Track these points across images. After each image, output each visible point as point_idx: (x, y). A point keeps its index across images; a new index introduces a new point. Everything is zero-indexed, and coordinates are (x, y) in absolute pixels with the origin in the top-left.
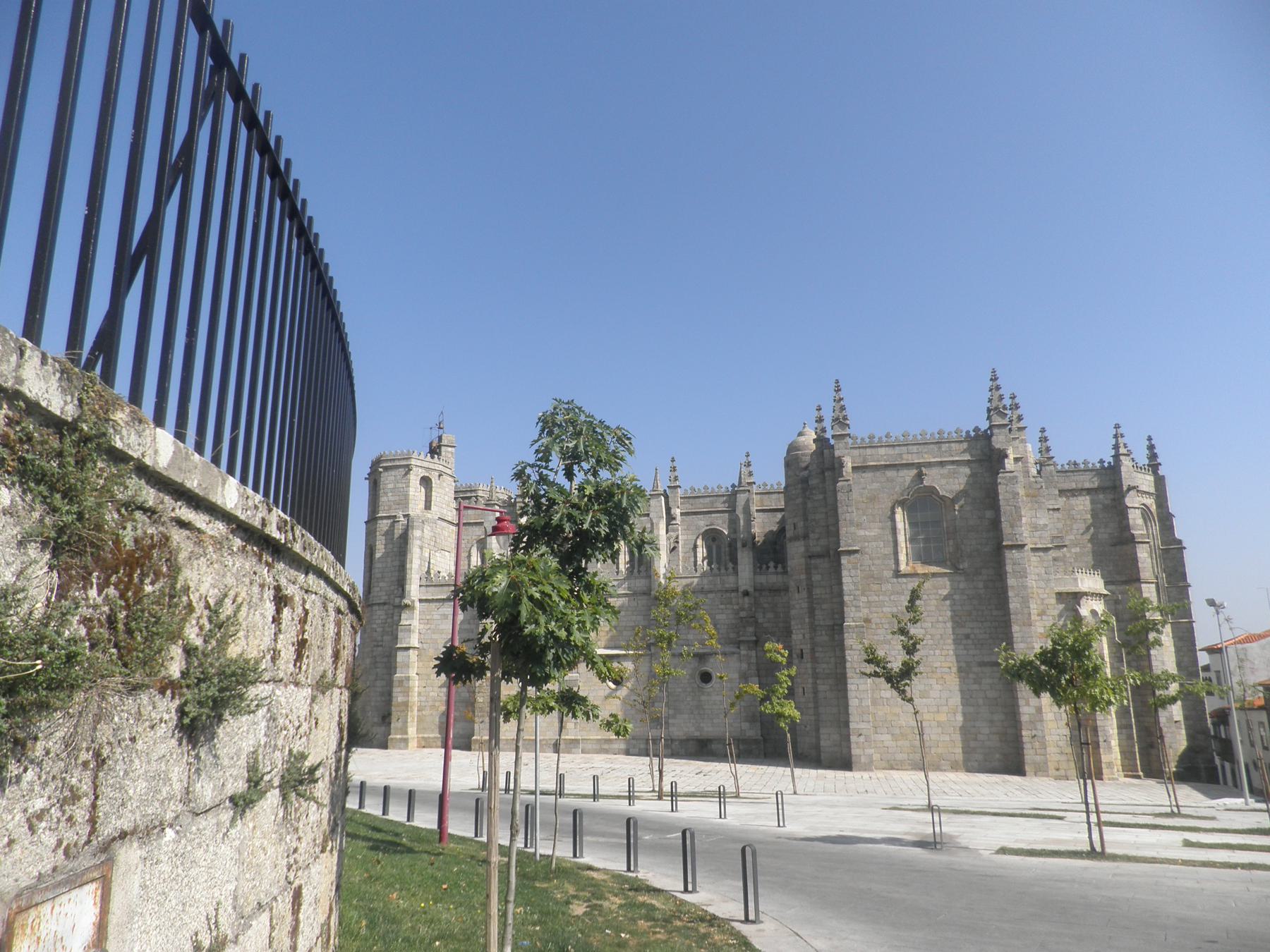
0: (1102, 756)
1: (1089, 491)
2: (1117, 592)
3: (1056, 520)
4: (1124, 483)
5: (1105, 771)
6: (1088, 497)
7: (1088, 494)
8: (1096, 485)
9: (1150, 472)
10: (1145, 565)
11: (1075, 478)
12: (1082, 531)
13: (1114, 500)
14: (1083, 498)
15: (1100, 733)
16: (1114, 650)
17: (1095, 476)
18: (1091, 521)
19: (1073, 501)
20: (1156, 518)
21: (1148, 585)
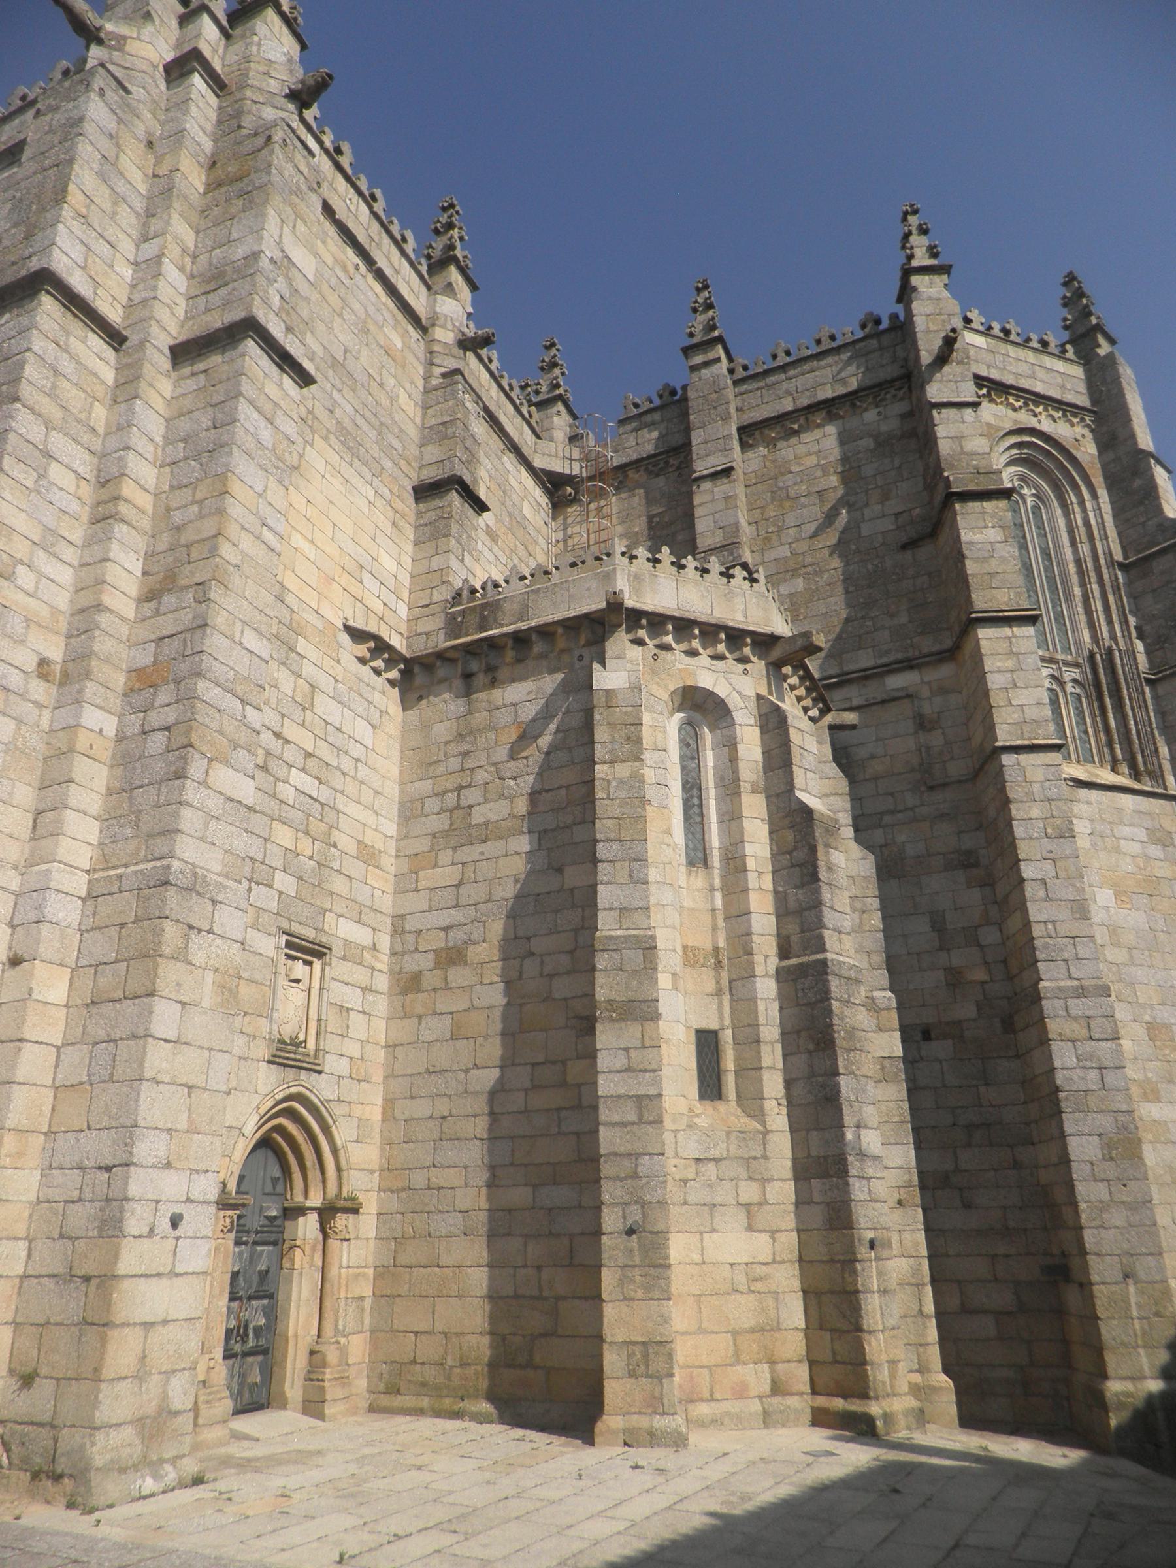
0: (610, 1311)
1: (829, 408)
2: (925, 692)
3: (721, 505)
4: (921, 344)
5: (615, 1390)
6: (831, 429)
7: (831, 417)
8: (853, 384)
9: (1070, 354)
10: (993, 566)
11: (791, 385)
12: (811, 528)
13: (904, 417)
14: (817, 433)
15: (610, 1192)
16: (789, 836)
17: (848, 363)
18: (841, 491)
19: (788, 450)
20: (1098, 481)
21: (1007, 631)
